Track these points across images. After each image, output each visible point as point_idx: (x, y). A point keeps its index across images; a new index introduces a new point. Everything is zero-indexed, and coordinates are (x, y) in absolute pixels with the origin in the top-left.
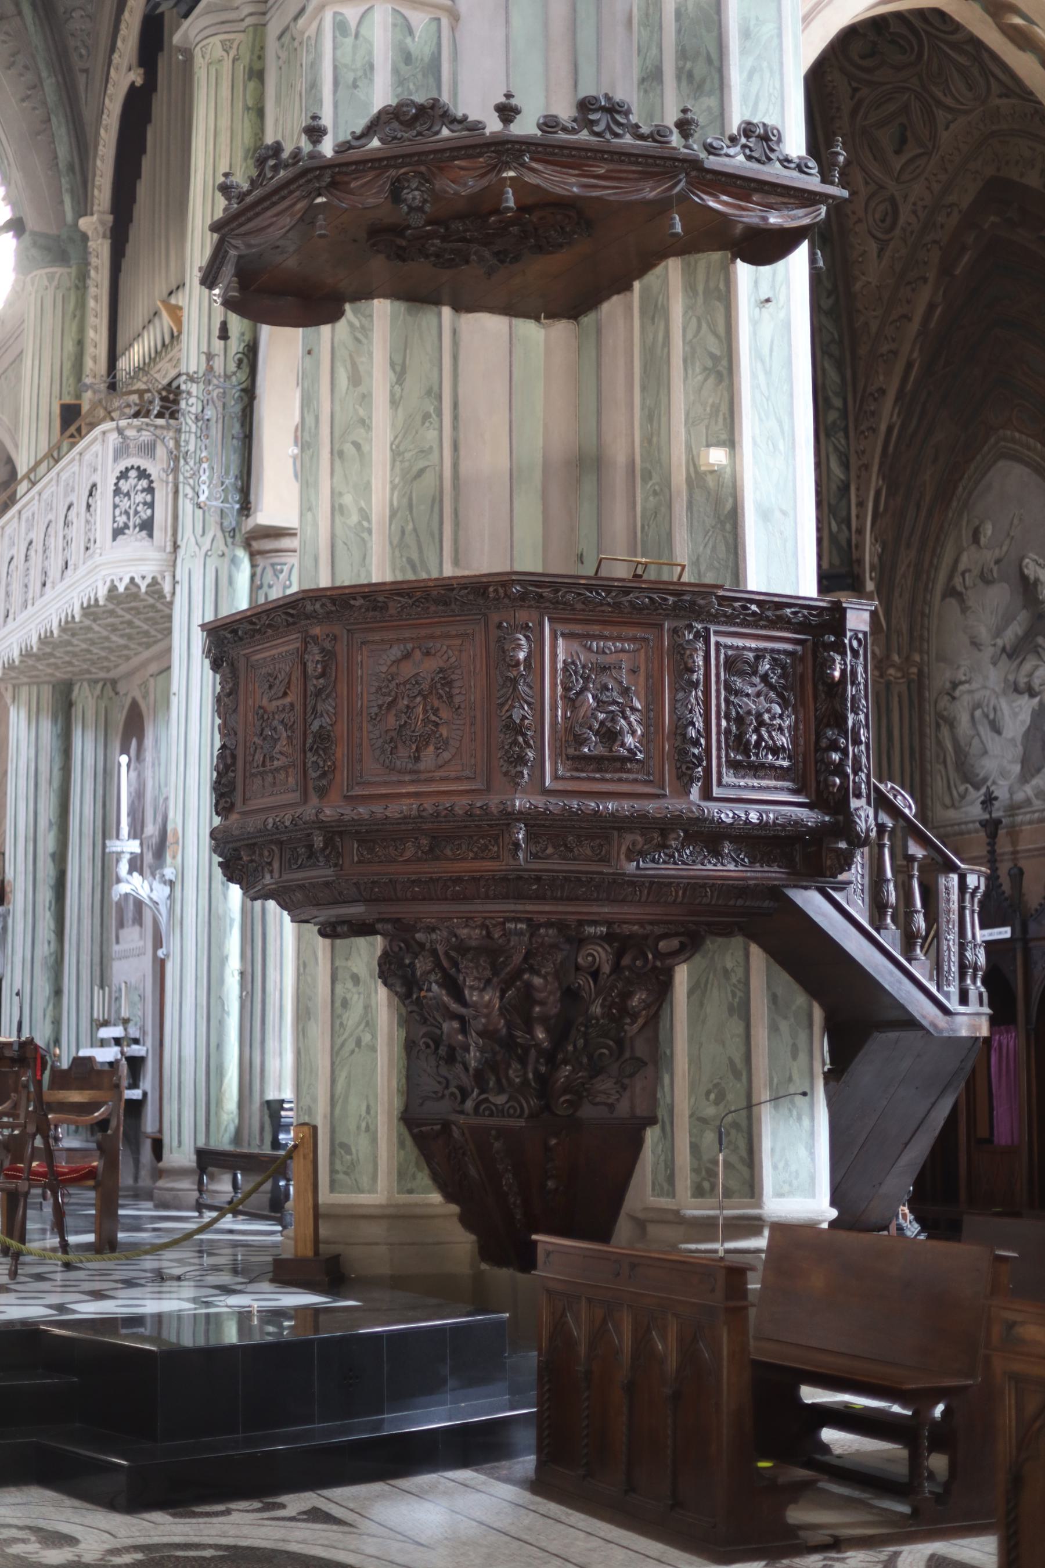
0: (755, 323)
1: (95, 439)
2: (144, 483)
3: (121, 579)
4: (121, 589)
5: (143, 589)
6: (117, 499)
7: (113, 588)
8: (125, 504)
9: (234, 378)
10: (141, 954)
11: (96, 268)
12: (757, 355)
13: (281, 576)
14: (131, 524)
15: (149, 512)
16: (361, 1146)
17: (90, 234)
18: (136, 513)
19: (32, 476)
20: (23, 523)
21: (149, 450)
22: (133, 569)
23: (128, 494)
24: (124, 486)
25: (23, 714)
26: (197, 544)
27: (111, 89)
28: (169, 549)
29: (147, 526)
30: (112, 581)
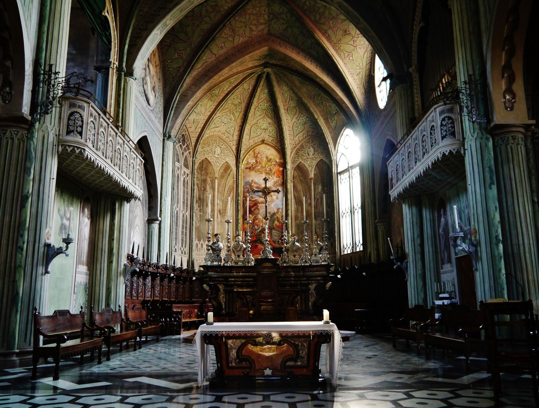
1: (432, 111)
2: (451, 121)
3: (447, 151)
4: (447, 154)
5: (454, 153)
6: (442, 127)
7: (444, 154)
8: (445, 128)
9: (479, 82)
10: (452, 271)
11: (416, 81)
13: (505, 141)
14: (448, 134)
15: (453, 129)
17: (412, 72)
18: (449, 130)
19: (401, 142)
20: (406, 148)
21: (451, 110)
22: (450, 147)
23: (446, 125)
24: (444, 123)
25: (407, 206)
26: (472, 136)
27: (414, 32)
28: (461, 140)
29: (453, 134)
30: (443, 152)
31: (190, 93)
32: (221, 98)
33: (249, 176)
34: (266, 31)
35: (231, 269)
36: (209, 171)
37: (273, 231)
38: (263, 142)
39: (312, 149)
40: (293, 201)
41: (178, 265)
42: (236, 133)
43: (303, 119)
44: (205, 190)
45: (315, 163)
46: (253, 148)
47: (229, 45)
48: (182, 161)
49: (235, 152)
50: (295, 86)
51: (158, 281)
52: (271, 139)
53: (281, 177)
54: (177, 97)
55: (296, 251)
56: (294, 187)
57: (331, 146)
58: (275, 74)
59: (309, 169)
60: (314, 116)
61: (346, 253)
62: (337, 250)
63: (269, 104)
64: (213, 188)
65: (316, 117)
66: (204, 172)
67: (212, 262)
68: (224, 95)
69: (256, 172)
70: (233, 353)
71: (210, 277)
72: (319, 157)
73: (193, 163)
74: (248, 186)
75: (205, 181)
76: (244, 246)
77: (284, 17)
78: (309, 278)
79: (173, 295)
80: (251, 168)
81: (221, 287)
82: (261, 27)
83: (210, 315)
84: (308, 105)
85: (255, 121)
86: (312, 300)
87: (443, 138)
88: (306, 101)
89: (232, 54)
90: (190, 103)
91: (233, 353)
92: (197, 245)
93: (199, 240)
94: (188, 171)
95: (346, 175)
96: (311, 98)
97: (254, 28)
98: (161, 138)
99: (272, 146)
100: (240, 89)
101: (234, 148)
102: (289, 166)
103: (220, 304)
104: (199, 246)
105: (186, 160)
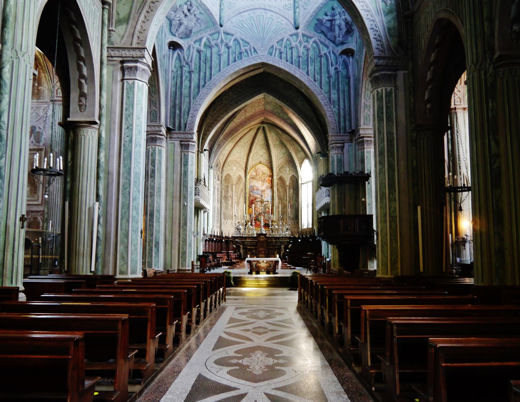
0: (368, 186)
12: (368, 189)
16: (335, 263)
31: (222, 143)
32: (237, 140)
33: (252, 182)
34: (263, 109)
35: (246, 238)
36: (230, 181)
37: (265, 214)
38: (260, 163)
39: (288, 169)
40: (277, 197)
41: (216, 234)
42: (245, 158)
43: (284, 151)
44: (228, 191)
45: (289, 176)
46: (254, 166)
47: (243, 117)
48: (217, 178)
49: (244, 169)
50: (279, 134)
51: (207, 242)
52: (265, 161)
53: (270, 183)
54: (216, 147)
55: (276, 230)
56: (278, 189)
57: (298, 168)
58: (268, 127)
59: (286, 180)
60: (289, 151)
61: (304, 228)
62: (300, 226)
63: (265, 142)
64: (232, 190)
65: (291, 151)
66: (227, 181)
67: (237, 235)
68: (239, 139)
69: (256, 180)
70: (254, 266)
71: (237, 242)
72: (293, 173)
73: (222, 177)
74: (252, 189)
75: (227, 187)
76: (252, 227)
77: (273, 104)
78: (281, 242)
79: (213, 250)
80: (253, 178)
81: (241, 246)
82: (260, 107)
83: (249, 256)
84: (286, 144)
85: (256, 151)
86: (282, 252)
87: (326, 196)
88: (285, 142)
89: (245, 121)
90: (222, 148)
91: (254, 266)
92: (224, 223)
93: (225, 220)
94: (219, 182)
95: (306, 184)
96: (288, 141)
97: (256, 108)
98: (208, 168)
99: (265, 165)
100: (248, 135)
101: (244, 166)
102: (275, 177)
103: (240, 254)
104: (225, 223)
105: (218, 176)
